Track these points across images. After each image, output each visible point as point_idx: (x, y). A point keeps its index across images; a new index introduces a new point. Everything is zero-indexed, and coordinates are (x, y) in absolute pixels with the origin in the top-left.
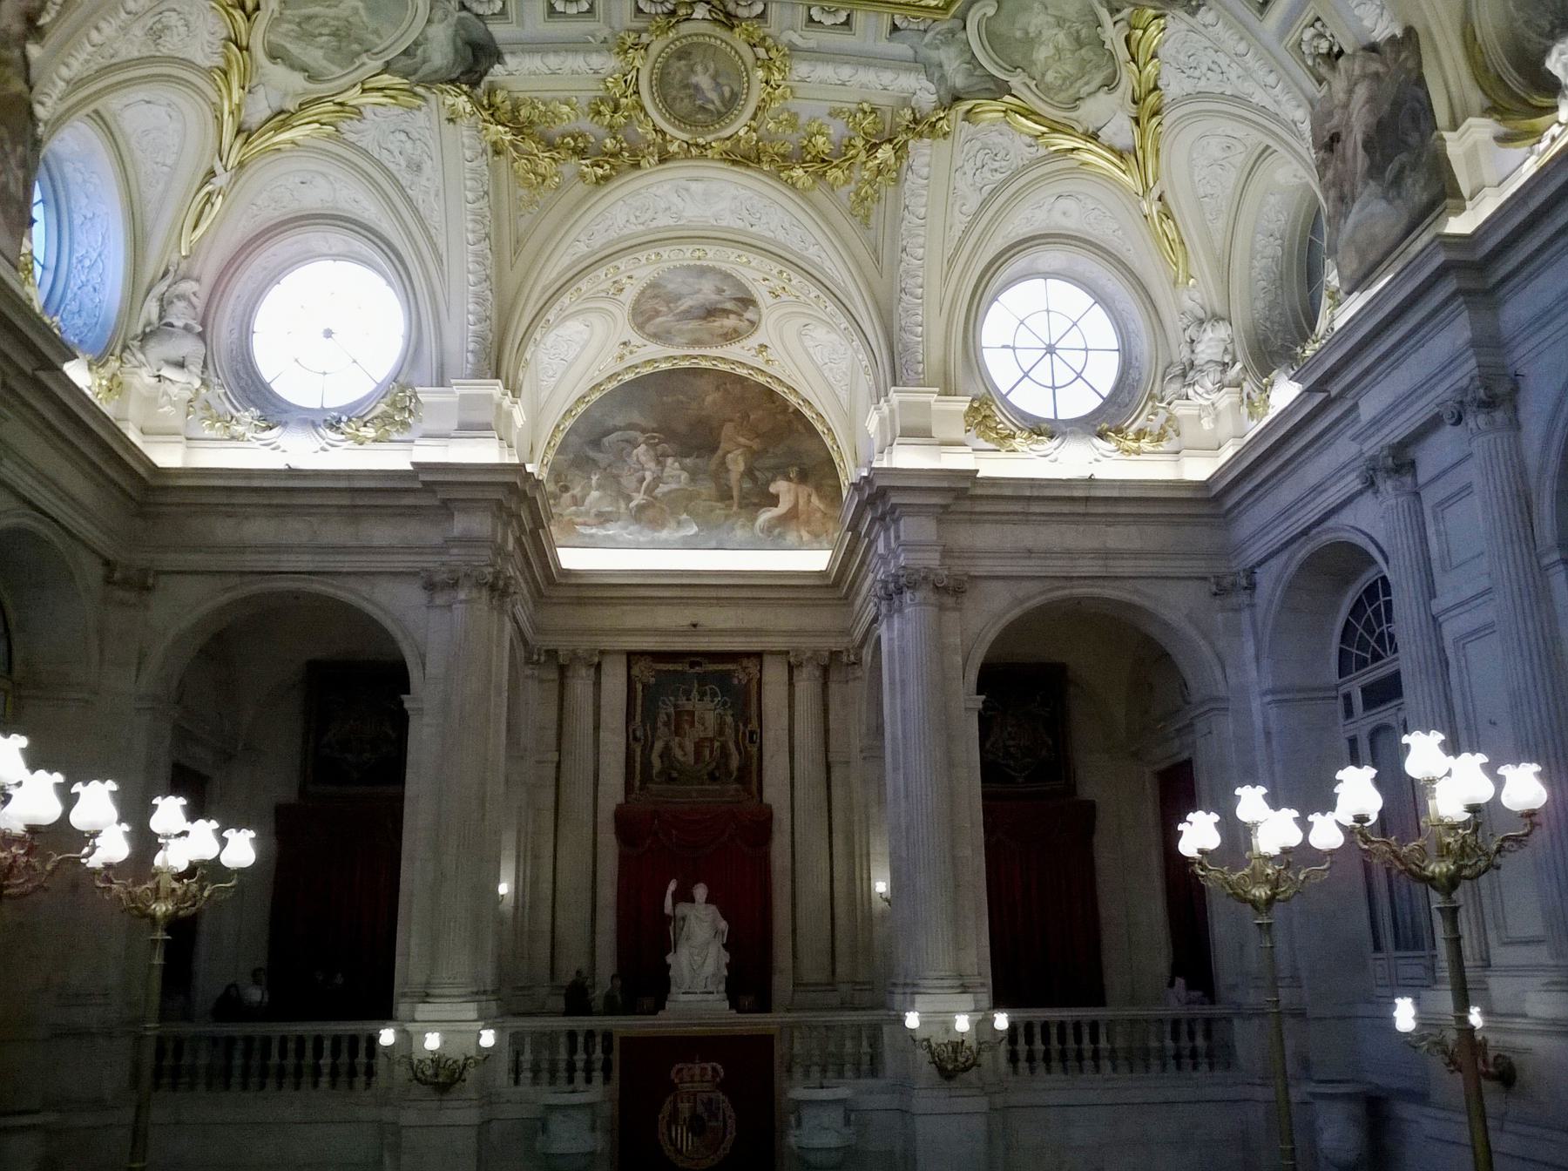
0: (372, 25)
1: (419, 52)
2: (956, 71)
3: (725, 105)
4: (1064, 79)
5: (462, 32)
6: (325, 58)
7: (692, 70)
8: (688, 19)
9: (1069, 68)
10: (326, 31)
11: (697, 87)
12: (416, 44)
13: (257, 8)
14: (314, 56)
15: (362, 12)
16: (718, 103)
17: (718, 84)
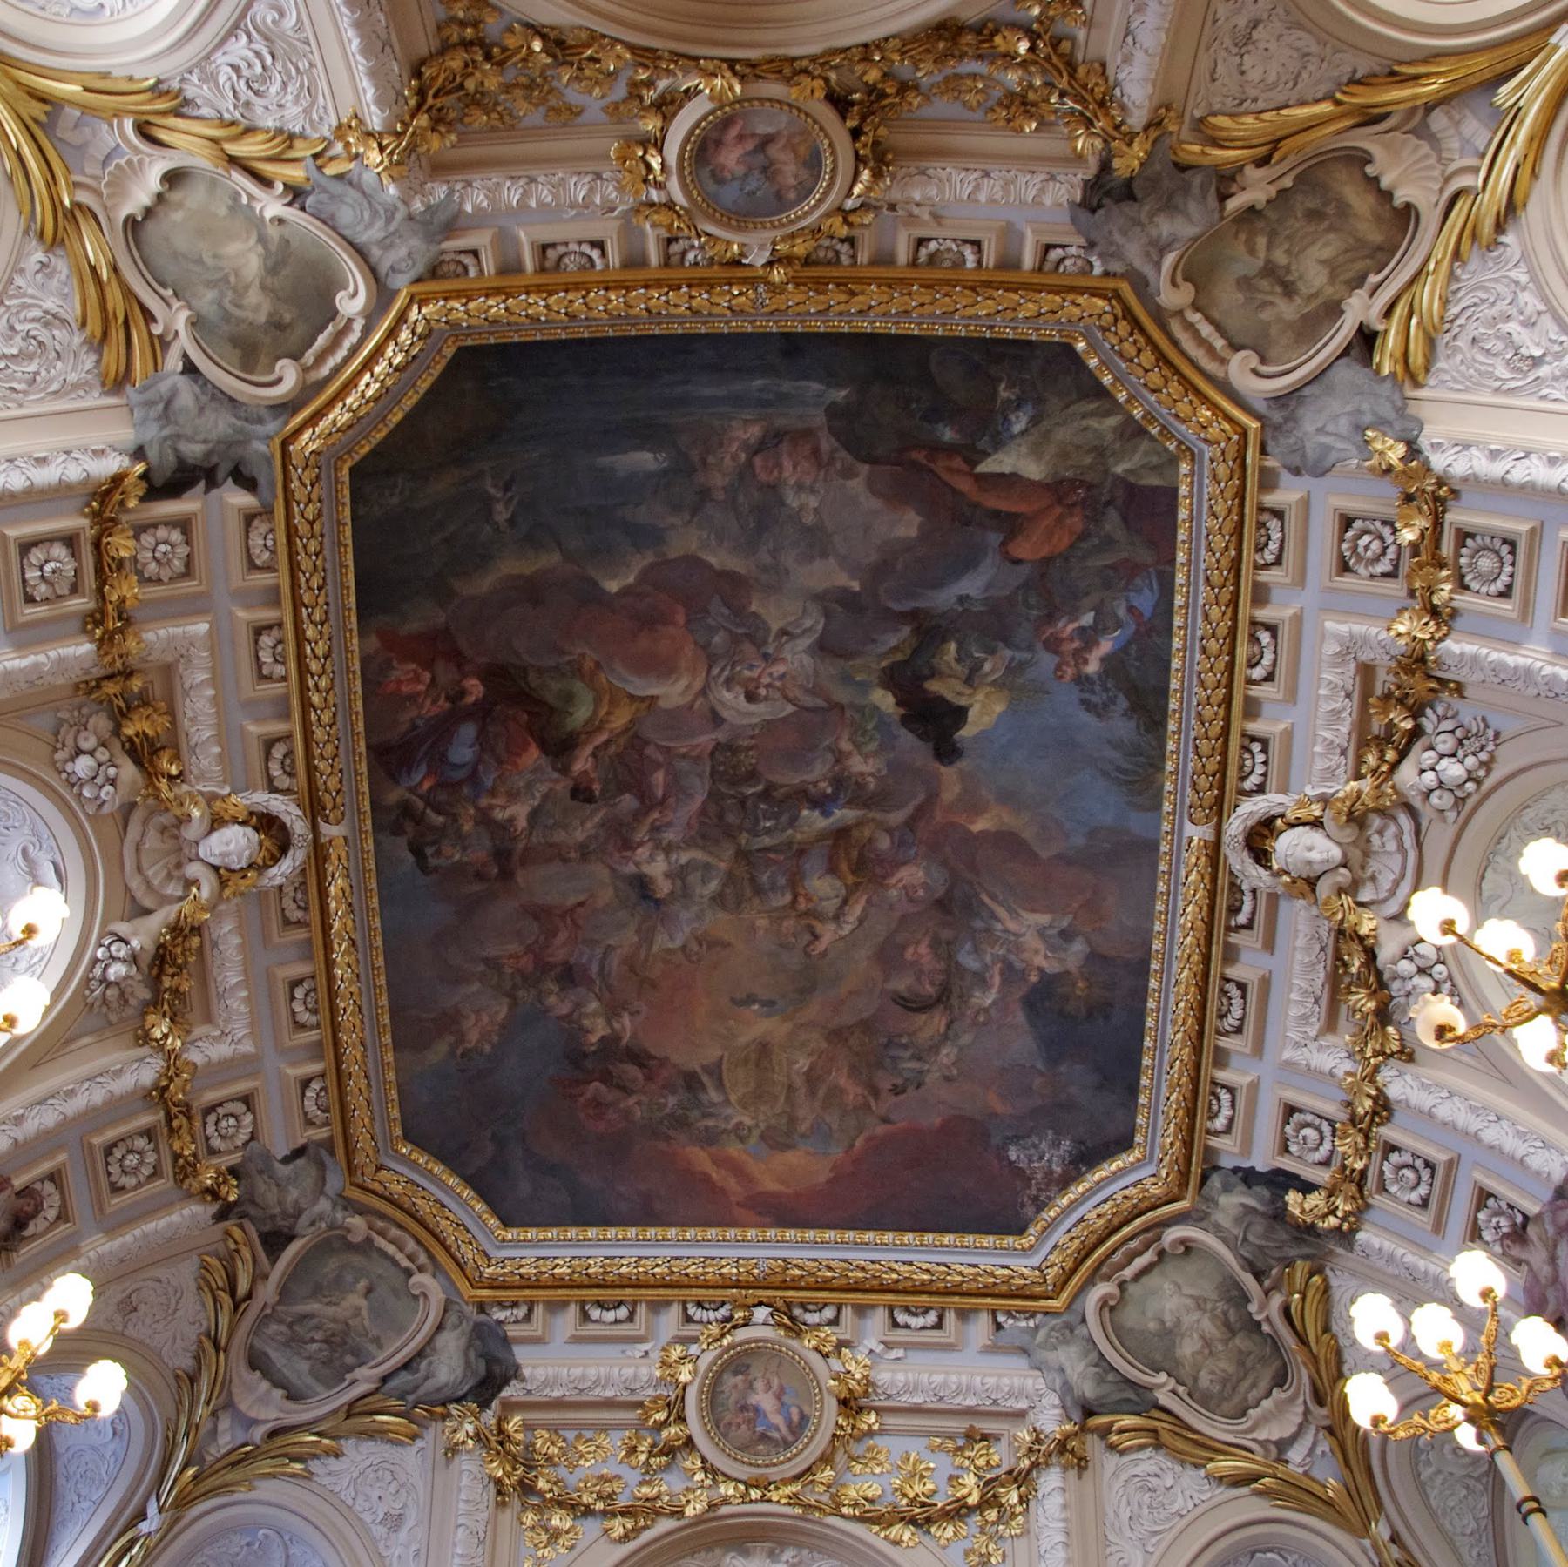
0: (374, 1332)
1: (423, 1365)
2: (1082, 1376)
3: (793, 1433)
4: (1224, 1382)
5: (478, 1343)
6: (312, 1372)
7: (750, 1386)
8: (747, 1322)
9: (1226, 1366)
10: (318, 1336)
11: (757, 1410)
12: (420, 1354)
13: (249, 1296)
14: (297, 1368)
15: (365, 1313)
16: (784, 1429)
17: (782, 1404)
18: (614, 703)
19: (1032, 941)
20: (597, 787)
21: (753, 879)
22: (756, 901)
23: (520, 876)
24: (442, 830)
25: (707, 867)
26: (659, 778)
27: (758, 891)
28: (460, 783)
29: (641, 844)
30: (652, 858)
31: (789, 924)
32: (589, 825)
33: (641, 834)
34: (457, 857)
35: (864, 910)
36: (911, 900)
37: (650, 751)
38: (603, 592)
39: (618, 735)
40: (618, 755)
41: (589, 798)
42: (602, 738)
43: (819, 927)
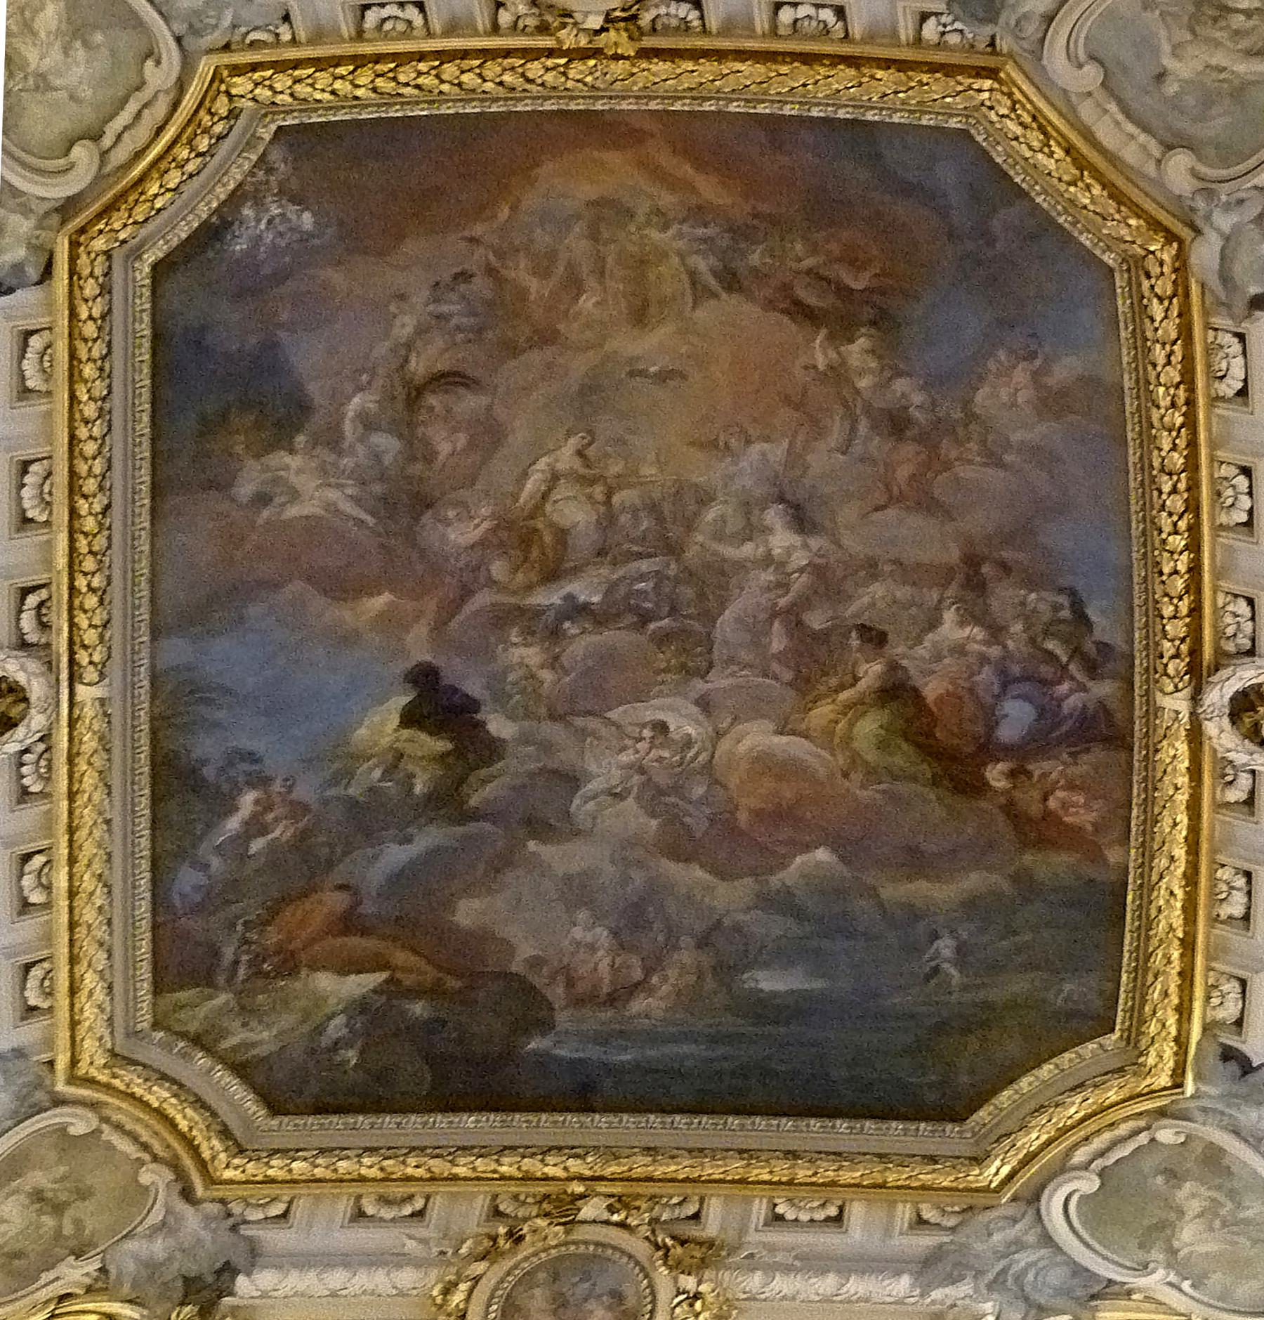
18: (829, 732)
19: (307, 483)
20: (855, 642)
21: (660, 519)
22: (656, 495)
23: (953, 554)
24: (1047, 633)
25: (719, 536)
26: (778, 642)
27: (653, 508)
28: (1018, 680)
29: (801, 570)
30: (789, 551)
31: (615, 468)
32: (866, 599)
33: (800, 583)
34: (1033, 596)
35: (521, 490)
36: (464, 504)
37: (788, 676)
38: (834, 851)
39: (827, 696)
40: (826, 674)
41: (864, 630)
42: (844, 696)
43: (577, 464)
